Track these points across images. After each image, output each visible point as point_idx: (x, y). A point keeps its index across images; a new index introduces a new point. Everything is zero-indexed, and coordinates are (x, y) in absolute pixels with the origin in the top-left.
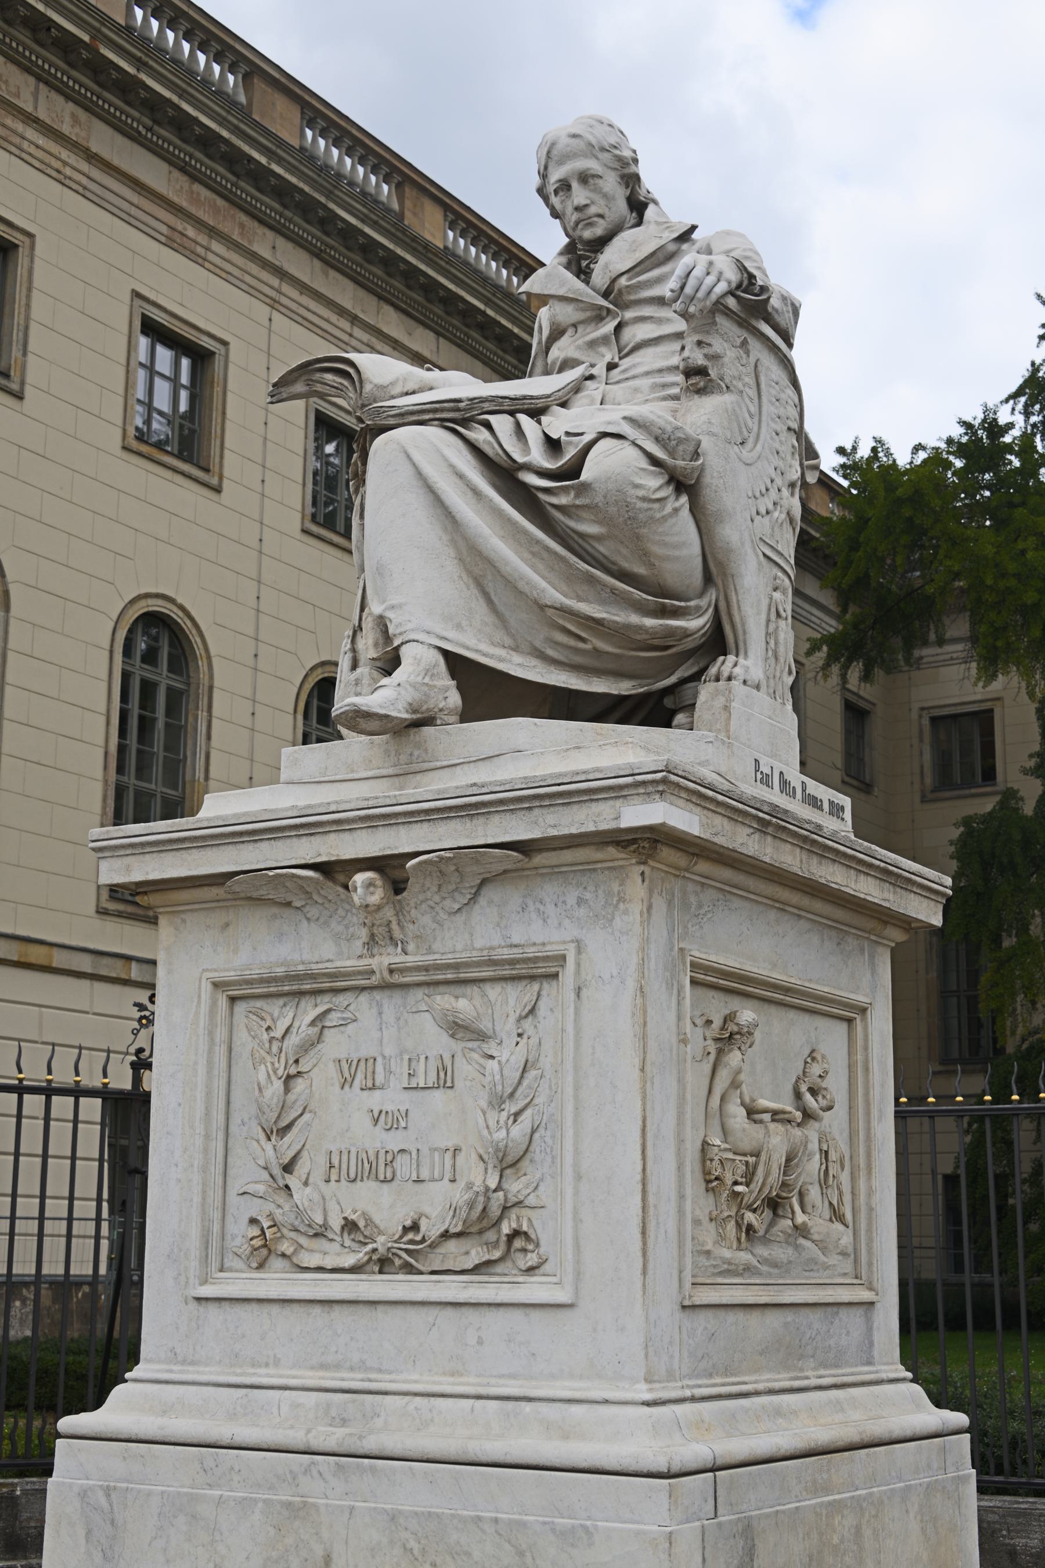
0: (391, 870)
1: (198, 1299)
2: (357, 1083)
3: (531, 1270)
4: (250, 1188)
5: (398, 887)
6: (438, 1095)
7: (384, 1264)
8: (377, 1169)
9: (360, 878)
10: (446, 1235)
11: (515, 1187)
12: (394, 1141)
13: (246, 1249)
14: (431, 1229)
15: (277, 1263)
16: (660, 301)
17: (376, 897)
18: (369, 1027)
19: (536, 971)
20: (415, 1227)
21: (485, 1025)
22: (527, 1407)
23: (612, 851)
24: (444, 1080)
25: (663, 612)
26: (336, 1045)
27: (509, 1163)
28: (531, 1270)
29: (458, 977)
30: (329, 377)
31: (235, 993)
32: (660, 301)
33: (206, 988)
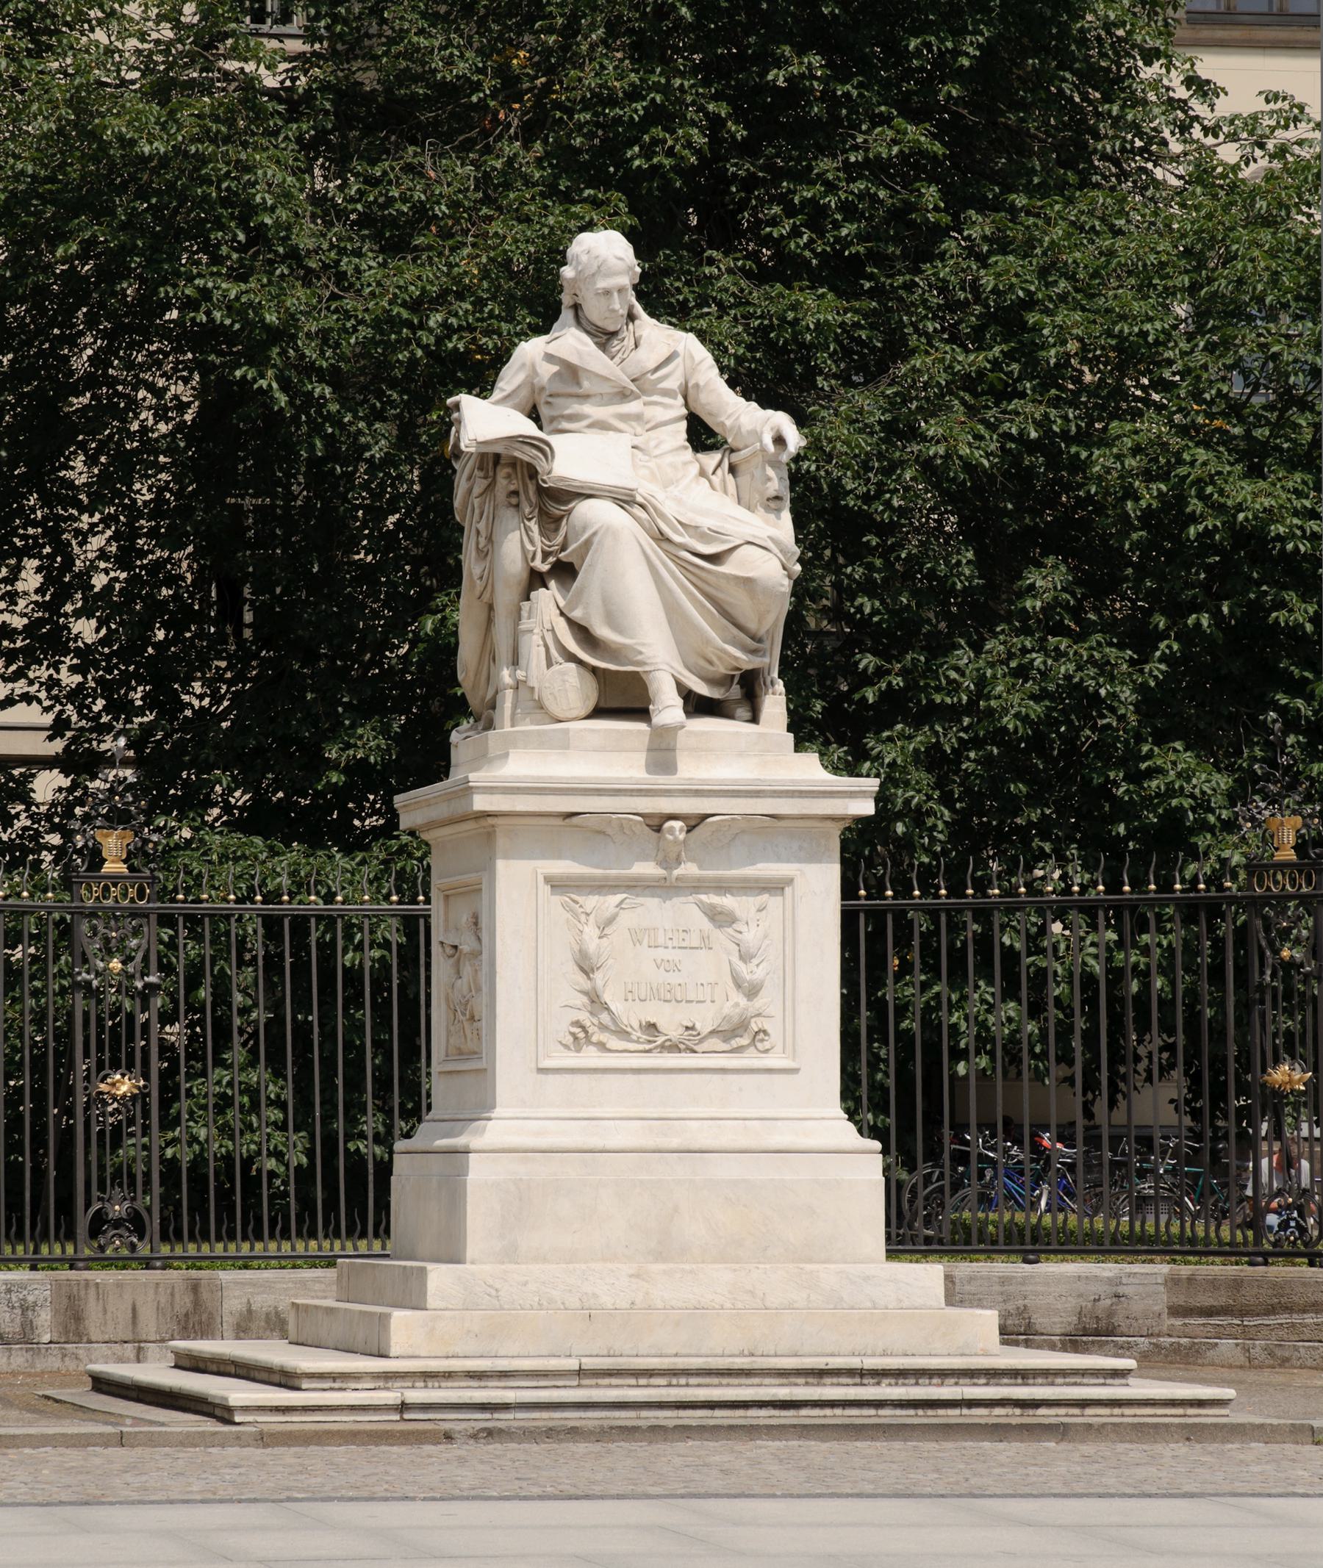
0: (694, 822)
1: (541, 1071)
2: (645, 942)
3: (766, 1051)
4: (571, 1003)
5: (690, 829)
6: (703, 952)
7: (673, 1048)
8: (670, 997)
9: (677, 825)
10: (713, 1032)
11: (759, 1003)
12: (674, 978)
13: (569, 1040)
14: (704, 1027)
15: (592, 1048)
16: (667, 393)
17: (682, 836)
18: (651, 910)
19: (776, 887)
20: (693, 1028)
21: (738, 913)
22: (779, 1123)
23: (829, 824)
24: (706, 943)
25: (754, 652)
26: (626, 919)
27: (752, 991)
28: (766, 1051)
29: (722, 887)
30: (527, 448)
31: (558, 885)
32: (667, 393)
33: (541, 879)
